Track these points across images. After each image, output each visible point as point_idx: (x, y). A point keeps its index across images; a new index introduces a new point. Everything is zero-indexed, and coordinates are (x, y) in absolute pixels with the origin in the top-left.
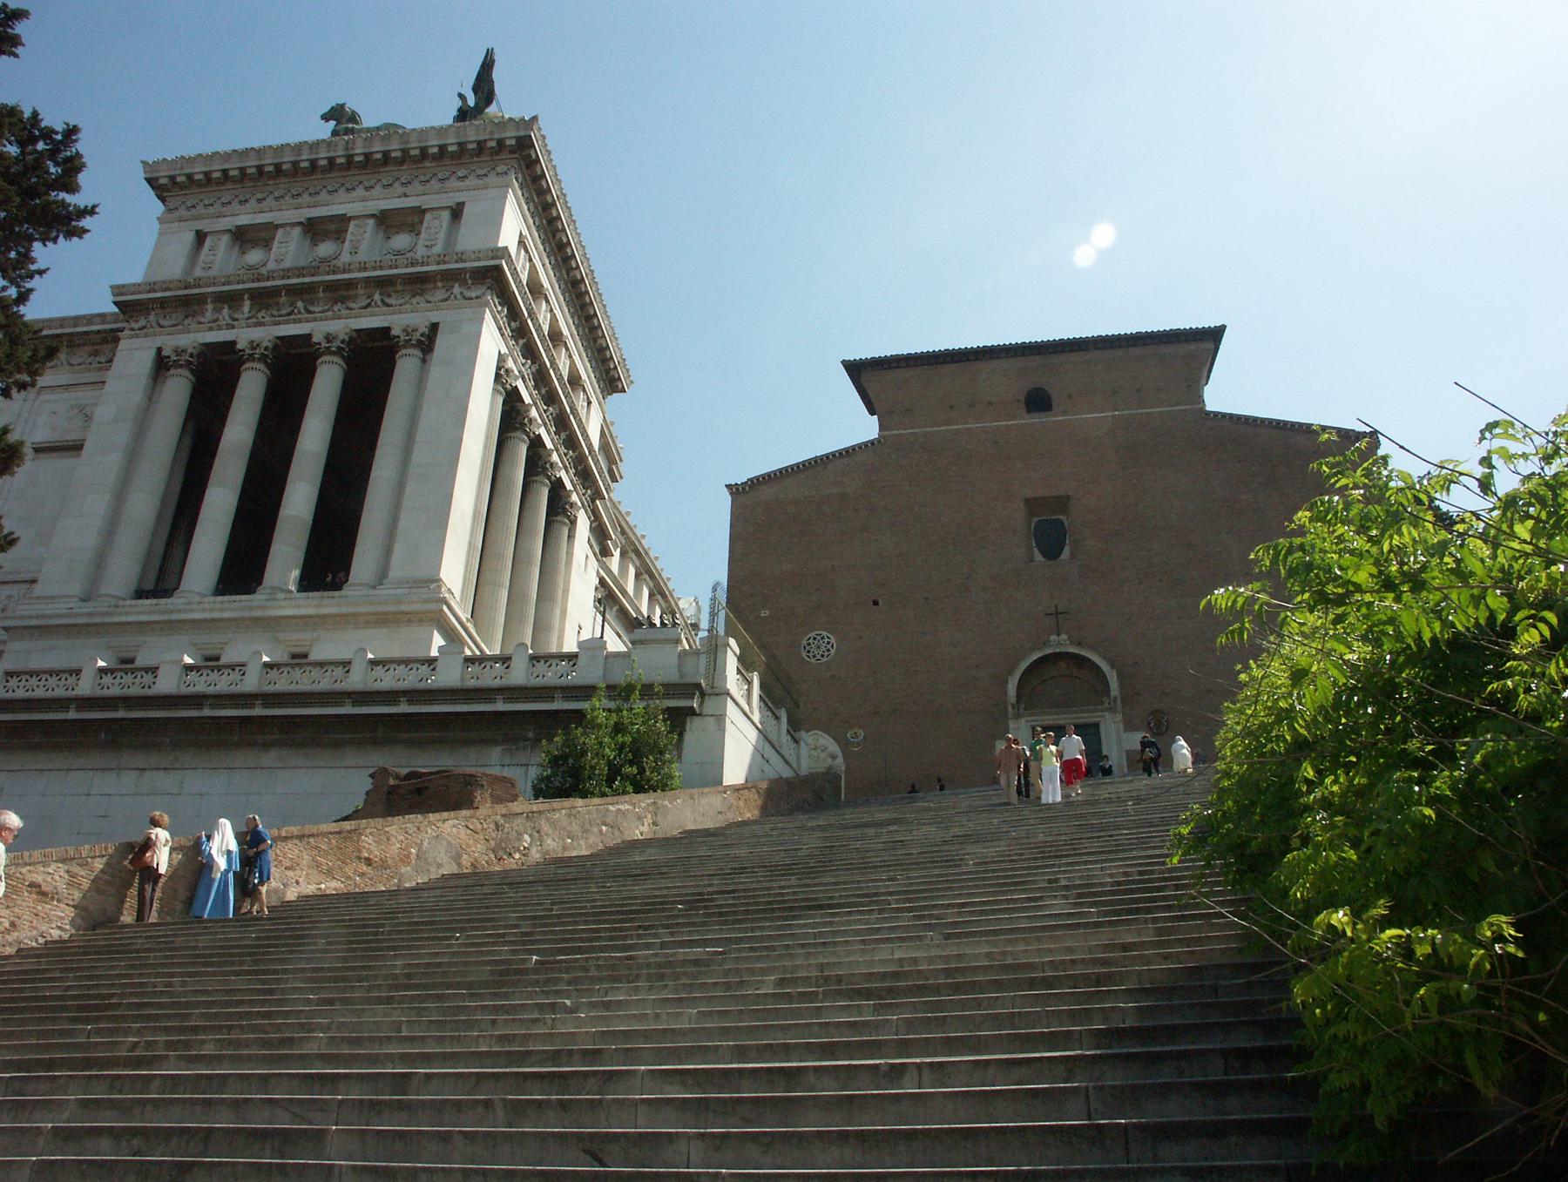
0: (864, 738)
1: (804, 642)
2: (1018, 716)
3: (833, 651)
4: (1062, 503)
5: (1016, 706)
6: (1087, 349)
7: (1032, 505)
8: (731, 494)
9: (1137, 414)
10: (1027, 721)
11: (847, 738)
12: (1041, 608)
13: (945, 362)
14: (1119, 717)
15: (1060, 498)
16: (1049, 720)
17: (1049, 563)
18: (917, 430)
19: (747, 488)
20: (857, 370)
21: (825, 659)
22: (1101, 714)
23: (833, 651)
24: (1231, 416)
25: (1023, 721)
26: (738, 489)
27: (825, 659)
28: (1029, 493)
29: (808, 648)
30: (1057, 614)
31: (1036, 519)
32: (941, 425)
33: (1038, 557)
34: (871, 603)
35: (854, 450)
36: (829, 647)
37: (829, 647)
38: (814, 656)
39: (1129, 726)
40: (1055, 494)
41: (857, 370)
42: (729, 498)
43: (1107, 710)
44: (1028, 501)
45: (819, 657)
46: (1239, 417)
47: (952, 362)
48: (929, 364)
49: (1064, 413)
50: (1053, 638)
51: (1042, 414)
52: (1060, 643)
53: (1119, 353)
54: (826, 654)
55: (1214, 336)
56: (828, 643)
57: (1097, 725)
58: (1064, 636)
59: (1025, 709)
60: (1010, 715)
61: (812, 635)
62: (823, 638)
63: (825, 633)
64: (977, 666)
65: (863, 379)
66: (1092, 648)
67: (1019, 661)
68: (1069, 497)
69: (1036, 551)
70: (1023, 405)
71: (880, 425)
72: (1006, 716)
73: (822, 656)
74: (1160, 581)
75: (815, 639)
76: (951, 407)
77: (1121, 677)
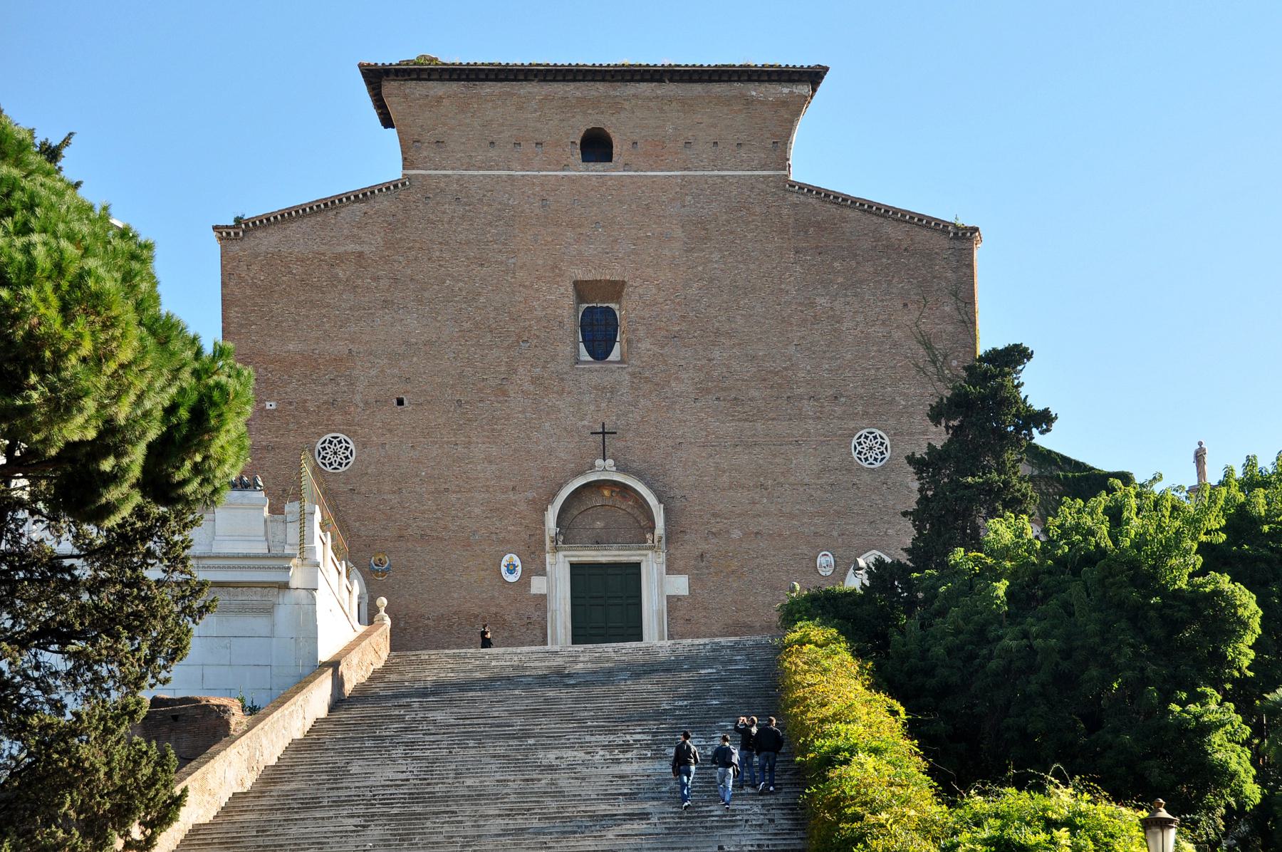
0: (390, 565)
1: (319, 446)
2: (556, 549)
3: (352, 459)
4: (616, 289)
5: (555, 540)
6: (661, 81)
7: (582, 290)
8: (221, 239)
9: (711, 176)
10: (565, 556)
11: (370, 565)
12: (586, 423)
13: (487, 79)
14: (663, 557)
15: (615, 283)
16: (587, 556)
17: (597, 366)
18: (450, 172)
19: (241, 234)
20: (375, 77)
21: (342, 469)
22: (644, 552)
23: (352, 459)
24: (819, 191)
25: (561, 554)
26: (228, 234)
27: (342, 469)
28: (580, 277)
29: (323, 453)
30: (604, 433)
31: (587, 305)
32: (480, 168)
33: (585, 355)
34: (395, 401)
35: (372, 192)
36: (348, 453)
37: (348, 453)
38: (331, 464)
39: (672, 568)
40: (608, 278)
41: (375, 77)
42: (216, 247)
43: (652, 548)
44: (576, 284)
45: (335, 465)
46: (827, 194)
47: (497, 80)
48: (468, 80)
49: (627, 166)
50: (599, 462)
51: (599, 166)
52: (606, 470)
53: (698, 89)
54: (344, 462)
55: (814, 76)
56: (347, 448)
57: (637, 566)
58: (610, 462)
59: (564, 543)
60: (547, 548)
61: (328, 437)
62: (340, 442)
63: (342, 436)
64: (514, 489)
65: (384, 91)
66: (639, 476)
67: (560, 487)
68: (624, 283)
69: (582, 346)
70: (578, 152)
71: (405, 159)
72: (544, 550)
73: (340, 464)
74: (718, 399)
75: (331, 442)
76: (492, 143)
77: (667, 512)
